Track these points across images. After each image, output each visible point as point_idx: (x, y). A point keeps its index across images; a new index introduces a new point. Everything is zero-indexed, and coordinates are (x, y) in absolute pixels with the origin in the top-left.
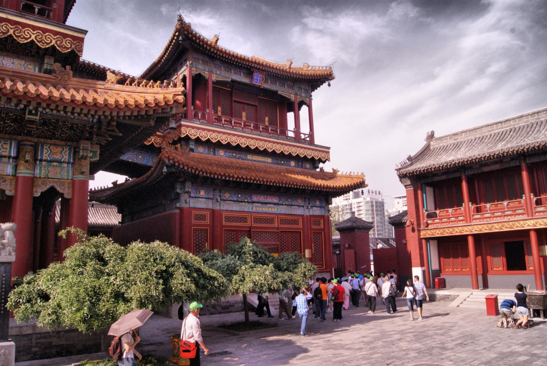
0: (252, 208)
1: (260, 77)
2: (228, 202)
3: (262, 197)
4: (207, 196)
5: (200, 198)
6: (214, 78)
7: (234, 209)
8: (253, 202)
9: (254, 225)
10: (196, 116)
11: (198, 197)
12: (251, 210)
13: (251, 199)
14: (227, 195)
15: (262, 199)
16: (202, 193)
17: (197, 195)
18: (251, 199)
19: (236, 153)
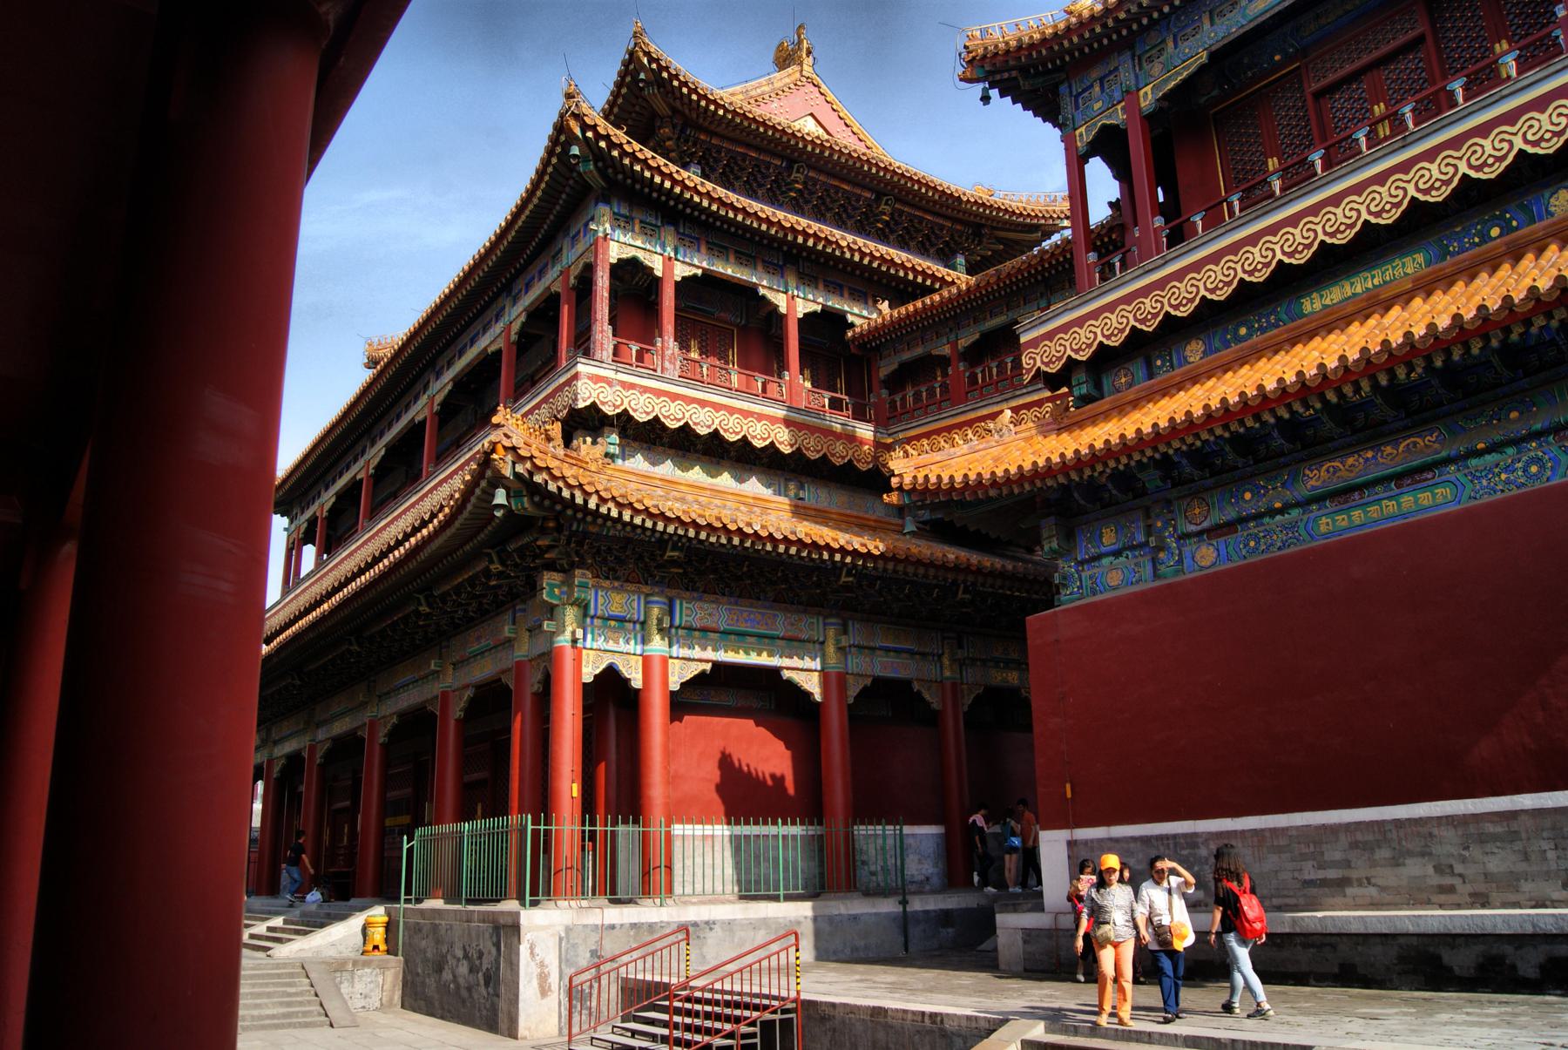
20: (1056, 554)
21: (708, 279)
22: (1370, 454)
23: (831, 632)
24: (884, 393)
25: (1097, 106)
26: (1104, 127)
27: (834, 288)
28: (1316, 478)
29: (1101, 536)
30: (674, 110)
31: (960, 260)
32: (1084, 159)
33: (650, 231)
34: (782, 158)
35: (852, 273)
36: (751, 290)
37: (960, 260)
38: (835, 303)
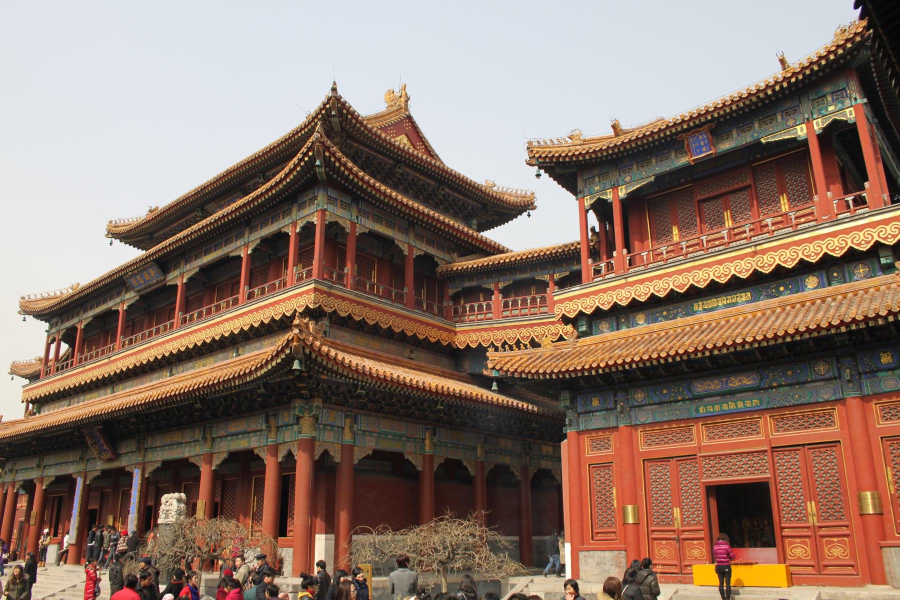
0: (697, 410)
1: (703, 140)
2: (648, 407)
3: (716, 381)
4: (604, 406)
5: (596, 411)
6: (622, 193)
7: (658, 420)
8: (700, 398)
9: (706, 442)
10: (597, 272)
11: (590, 412)
12: (694, 415)
13: (690, 391)
14: (640, 396)
15: (714, 385)
16: (595, 403)
17: (589, 408)
18: (690, 391)
19: (668, 311)
20: (567, 408)
21: (372, 234)
22: (724, 380)
23: (428, 435)
24: (451, 303)
25: (597, 188)
26: (599, 199)
27: (430, 243)
28: (700, 387)
29: (591, 402)
30: (343, 129)
31: (475, 222)
32: (587, 211)
33: (345, 206)
34: (392, 158)
35: (425, 228)
36: (389, 242)
37: (475, 222)
38: (431, 251)
